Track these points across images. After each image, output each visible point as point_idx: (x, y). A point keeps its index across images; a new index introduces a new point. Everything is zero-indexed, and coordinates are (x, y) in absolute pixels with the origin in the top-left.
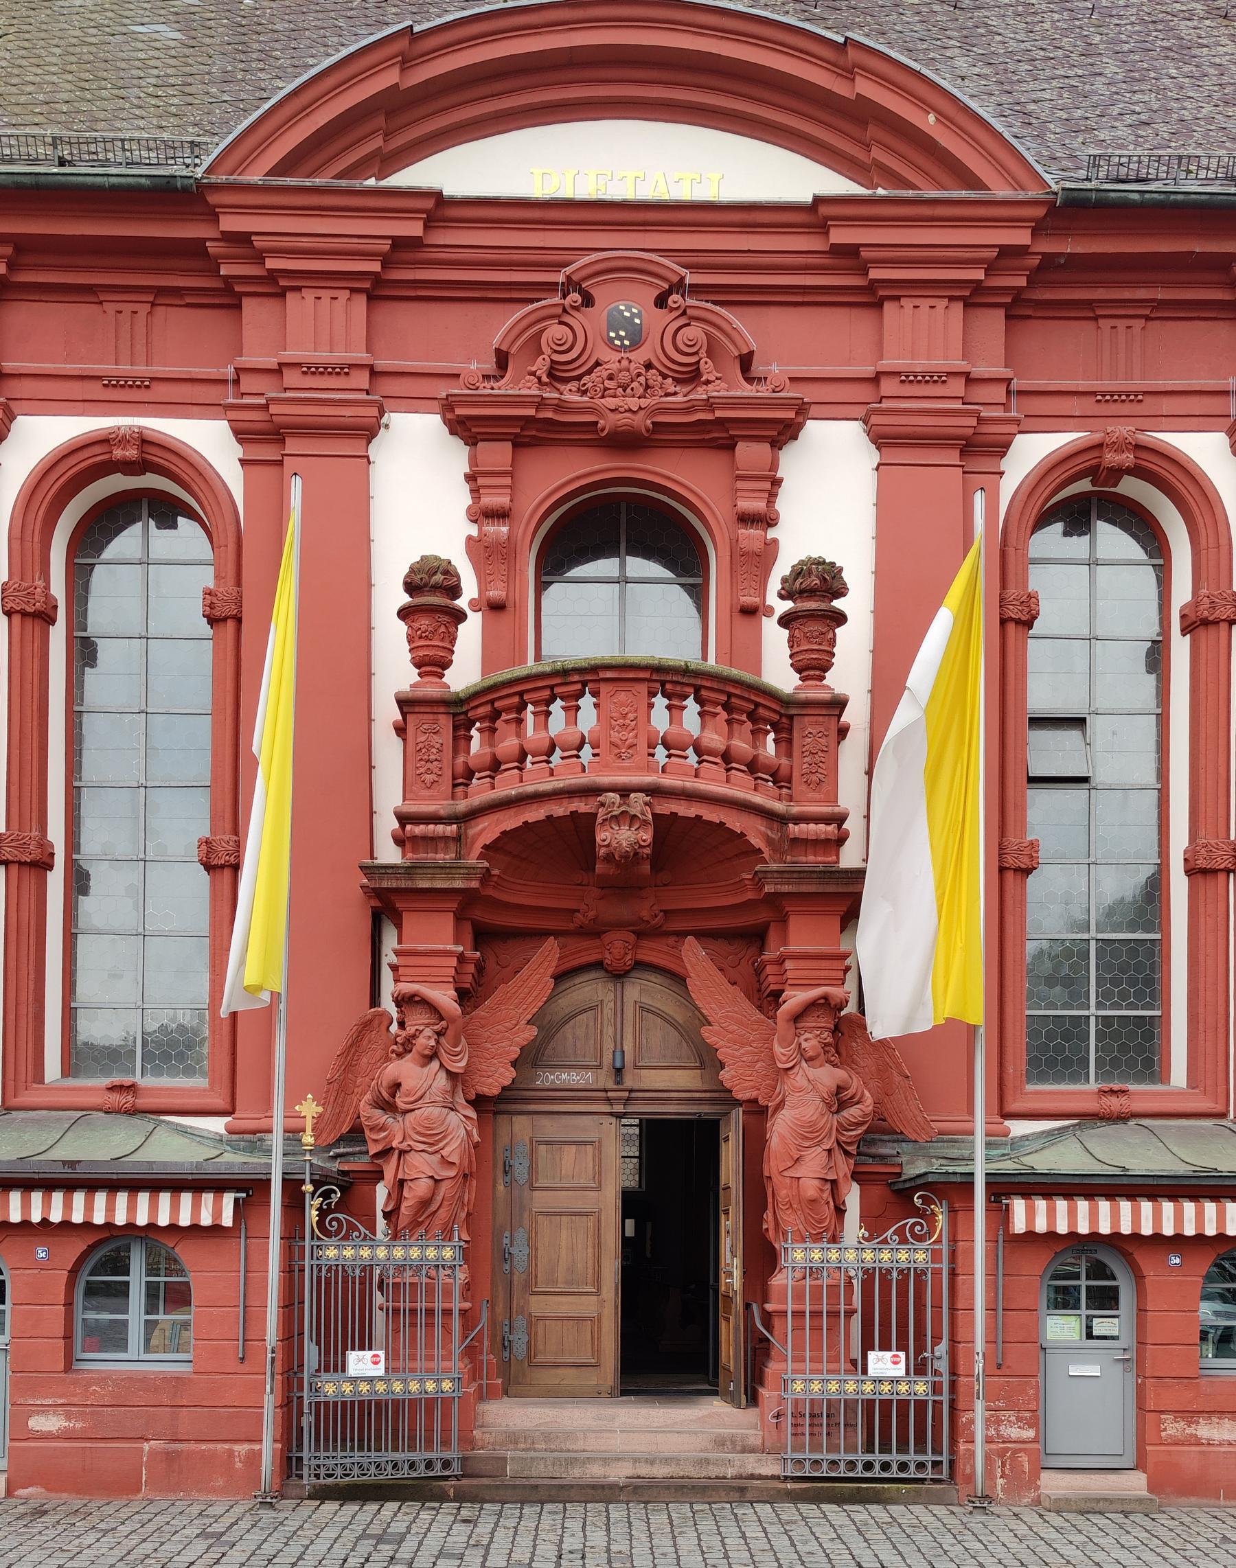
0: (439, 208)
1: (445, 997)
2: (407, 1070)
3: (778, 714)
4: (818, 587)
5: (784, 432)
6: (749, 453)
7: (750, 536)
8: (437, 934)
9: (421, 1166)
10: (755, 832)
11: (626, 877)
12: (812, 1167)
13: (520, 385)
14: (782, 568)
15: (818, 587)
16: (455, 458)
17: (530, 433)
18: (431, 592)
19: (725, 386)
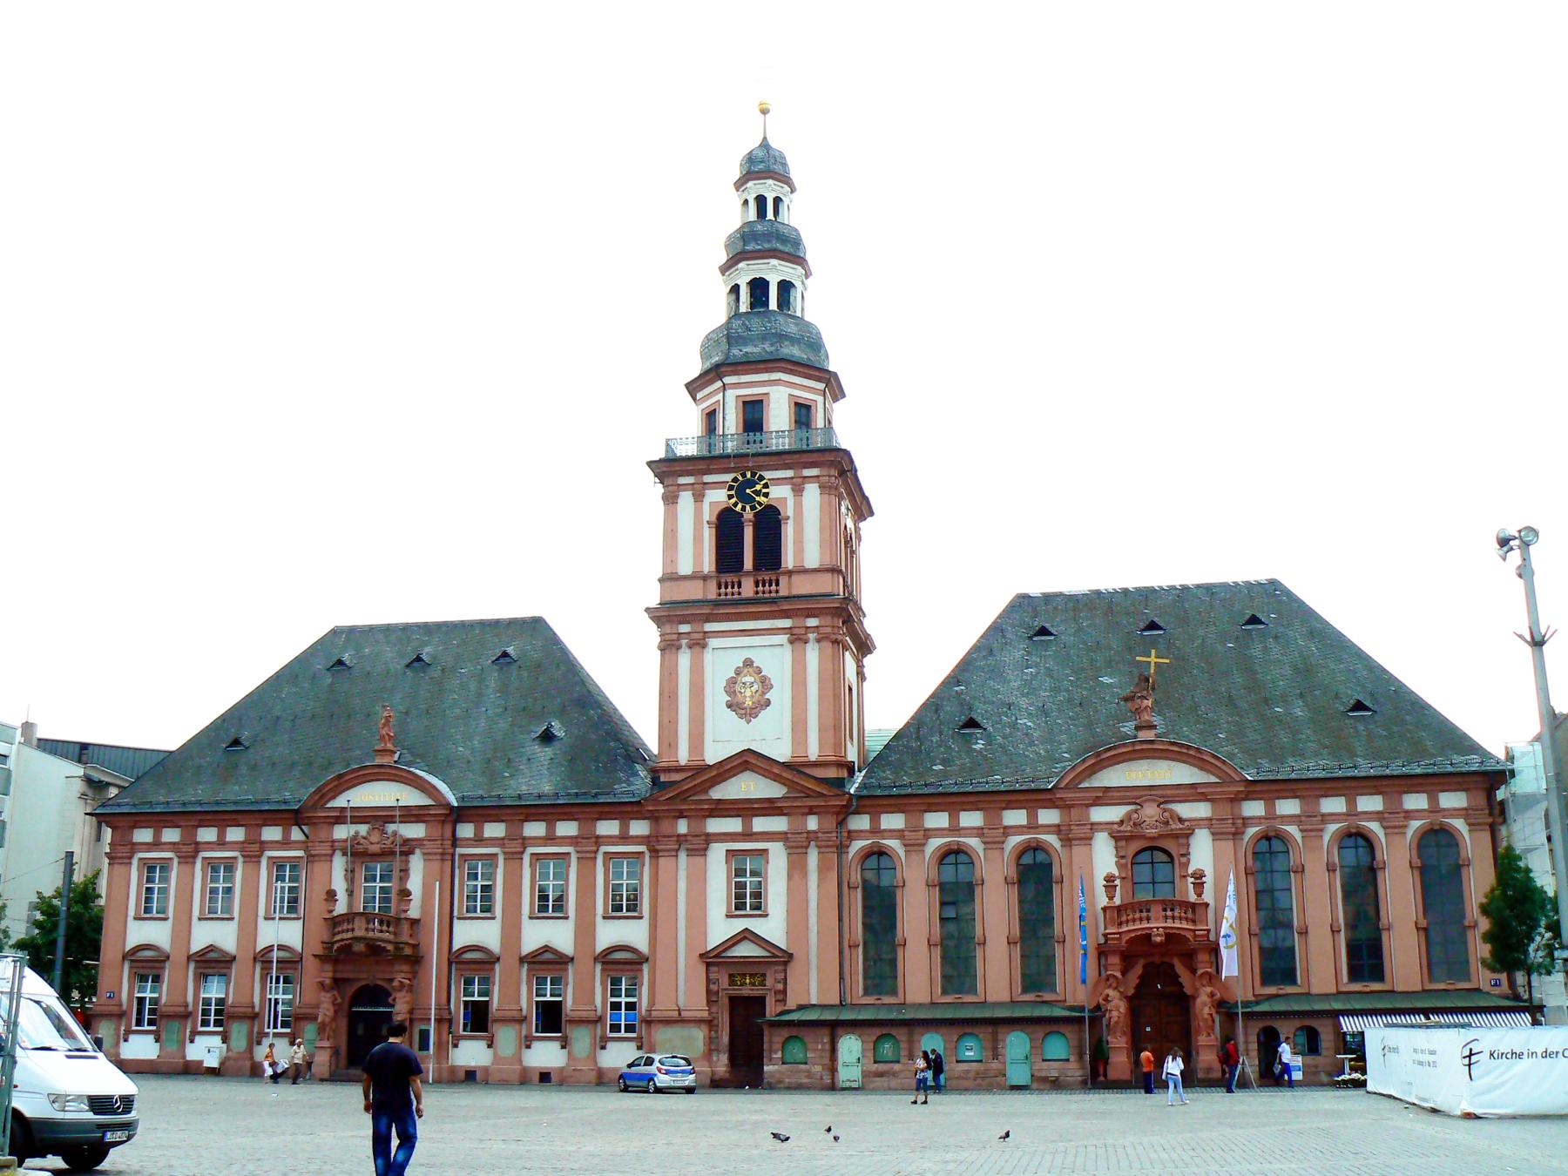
0: (1107, 789)
1: (1118, 975)
2: (1111, 992)
3: (1194, 906)
4: (1199, 875)
5: (1188, 836)
6: (1183, 841)
7: (1183, 860)
8: (1115, 960)
9: (1115, 1013)
10: (1189, 935)
11: (1160, 945)
12: (1206, 1010)
13: (1127, 828)
14: (1190, 871)
15: (1199, 875)
16: (1113, 843)
17: (1129, 838)
18: (1109, 879)
19: (1176, 826)
